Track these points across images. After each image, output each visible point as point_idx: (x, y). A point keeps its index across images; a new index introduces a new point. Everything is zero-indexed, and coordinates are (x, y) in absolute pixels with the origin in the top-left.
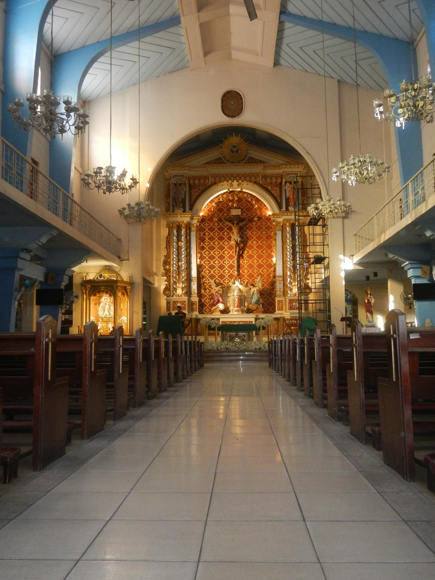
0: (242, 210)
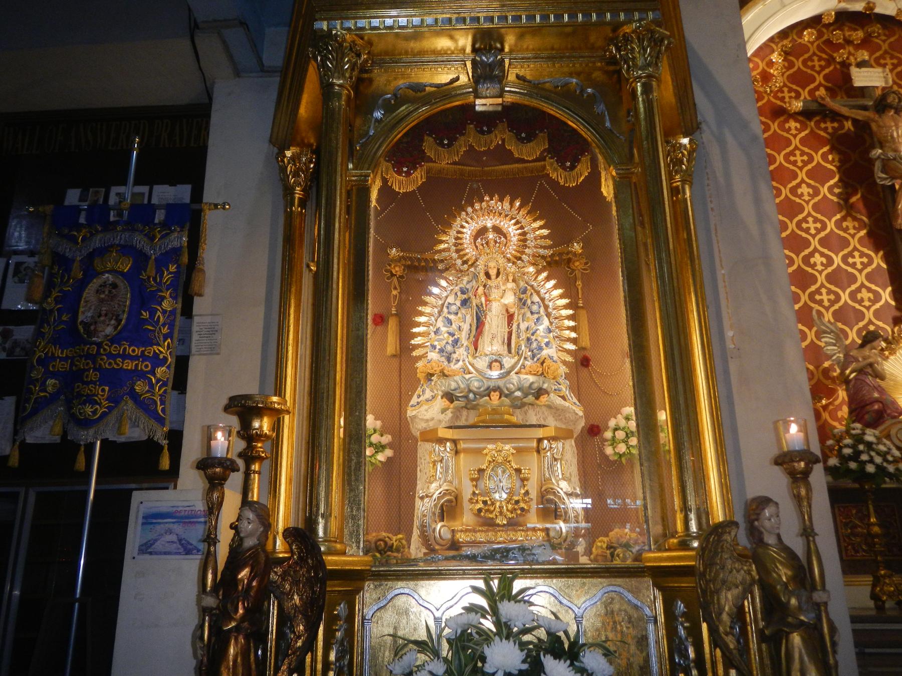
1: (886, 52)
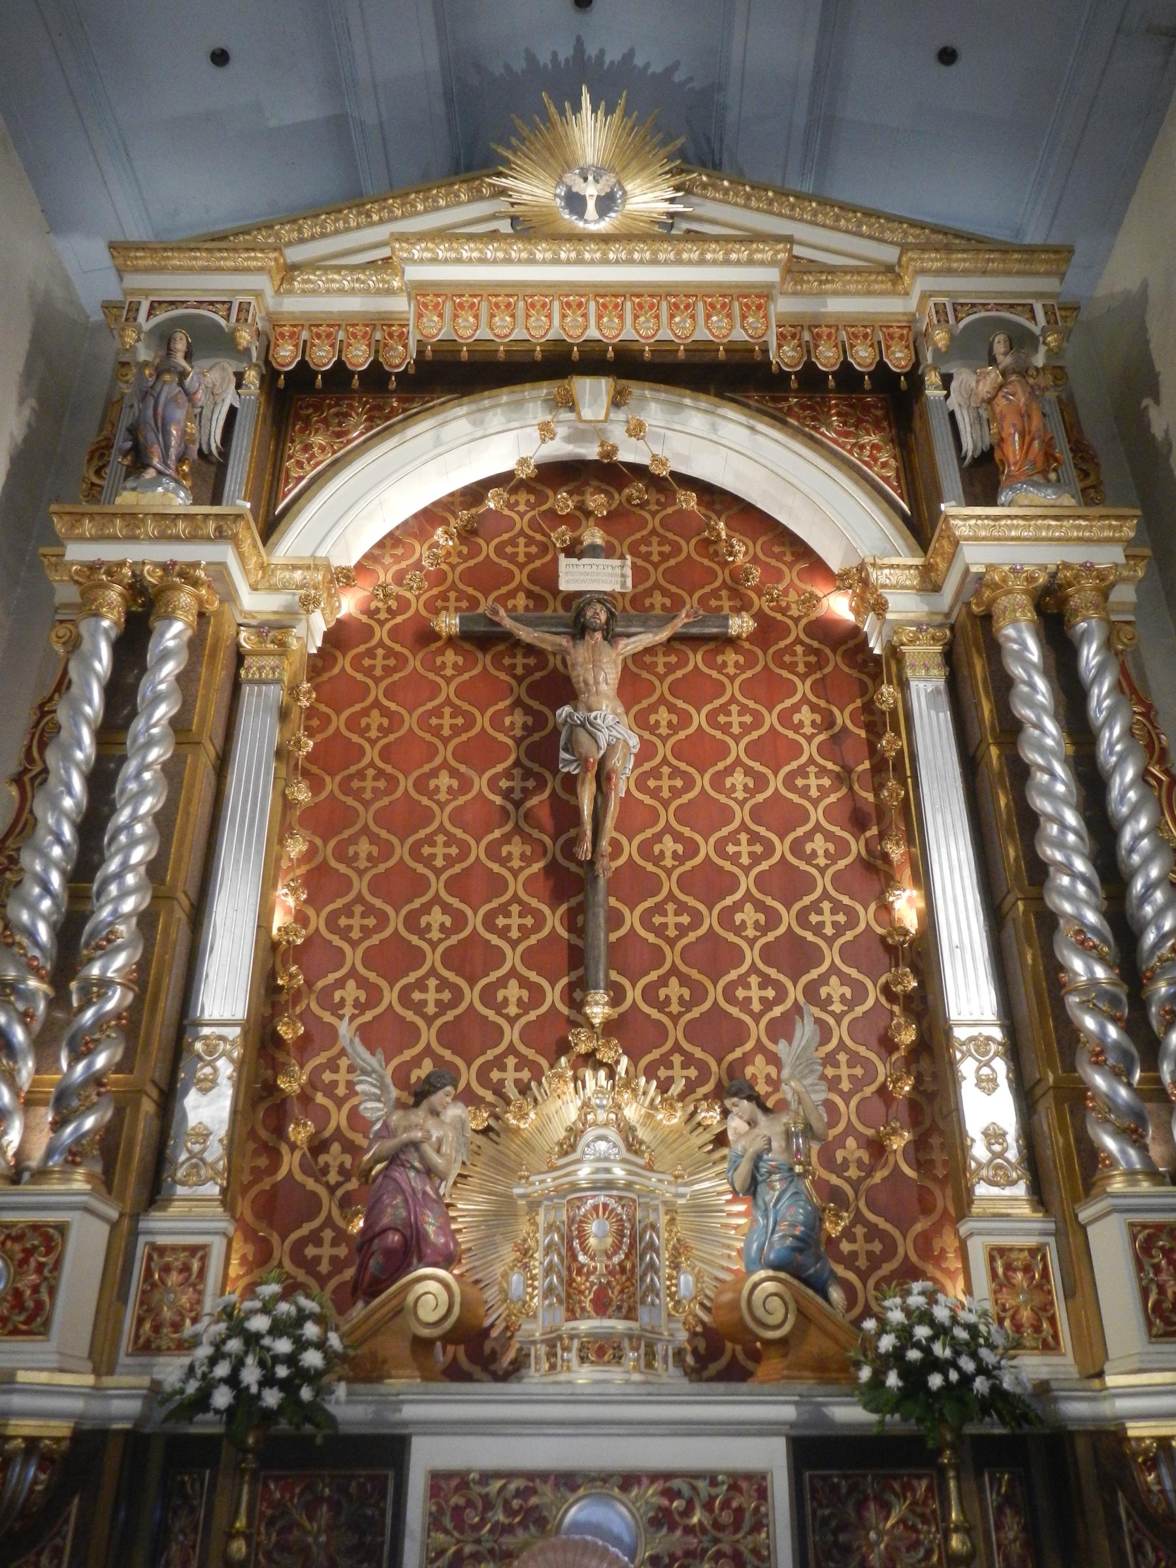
0: (639, 574)
1: (654, 532)
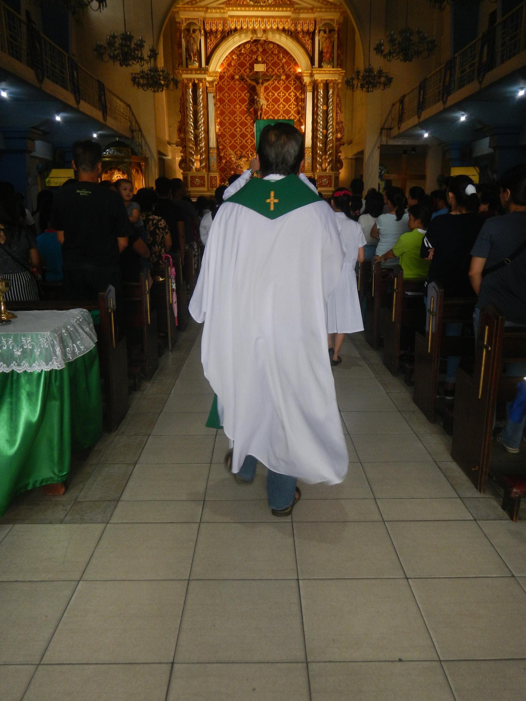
1: (270, 55)
